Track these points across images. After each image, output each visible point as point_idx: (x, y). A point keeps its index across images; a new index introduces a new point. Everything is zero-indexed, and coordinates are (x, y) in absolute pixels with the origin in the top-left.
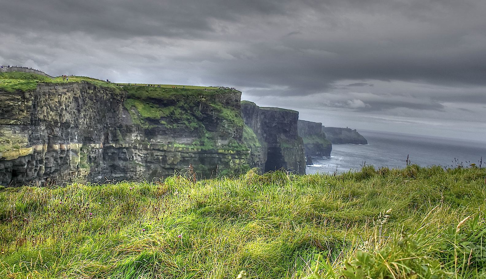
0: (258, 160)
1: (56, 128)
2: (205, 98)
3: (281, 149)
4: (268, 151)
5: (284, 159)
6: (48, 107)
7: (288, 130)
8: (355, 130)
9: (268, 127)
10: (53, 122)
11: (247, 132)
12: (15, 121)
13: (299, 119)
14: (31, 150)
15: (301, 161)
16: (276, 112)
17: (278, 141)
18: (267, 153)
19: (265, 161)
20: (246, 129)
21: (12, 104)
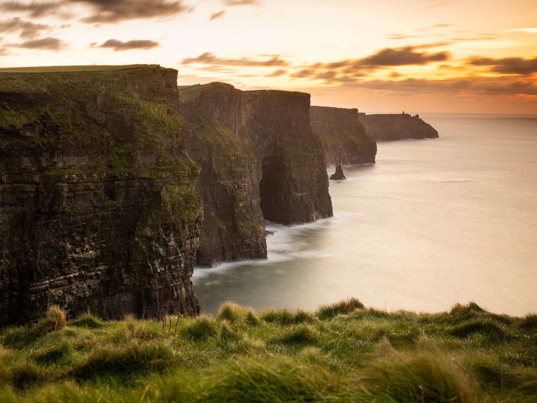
2: (106, 86)
4: (262, 162)
5: (290, 174)
7: (294, 125)
8: (417, 116)
11: (221, 136)
13: (311, 105)
17: (279, 144)
18: (261, 165)
19: (258, 179)
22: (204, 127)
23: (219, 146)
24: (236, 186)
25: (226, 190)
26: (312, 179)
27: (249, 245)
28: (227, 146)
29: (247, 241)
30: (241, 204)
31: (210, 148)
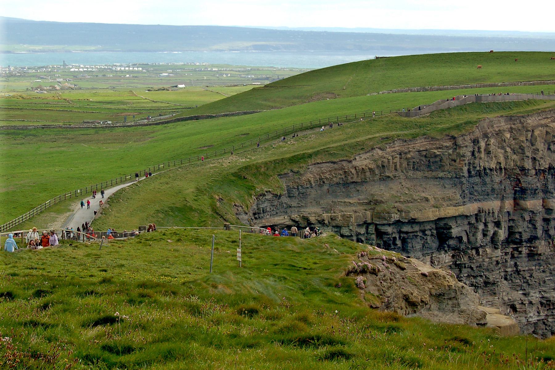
1: (525, 177)
6: (508, 149)
10: (518, 170)
12: (445, 173)
14: (471, 208)
21: (438, 153)
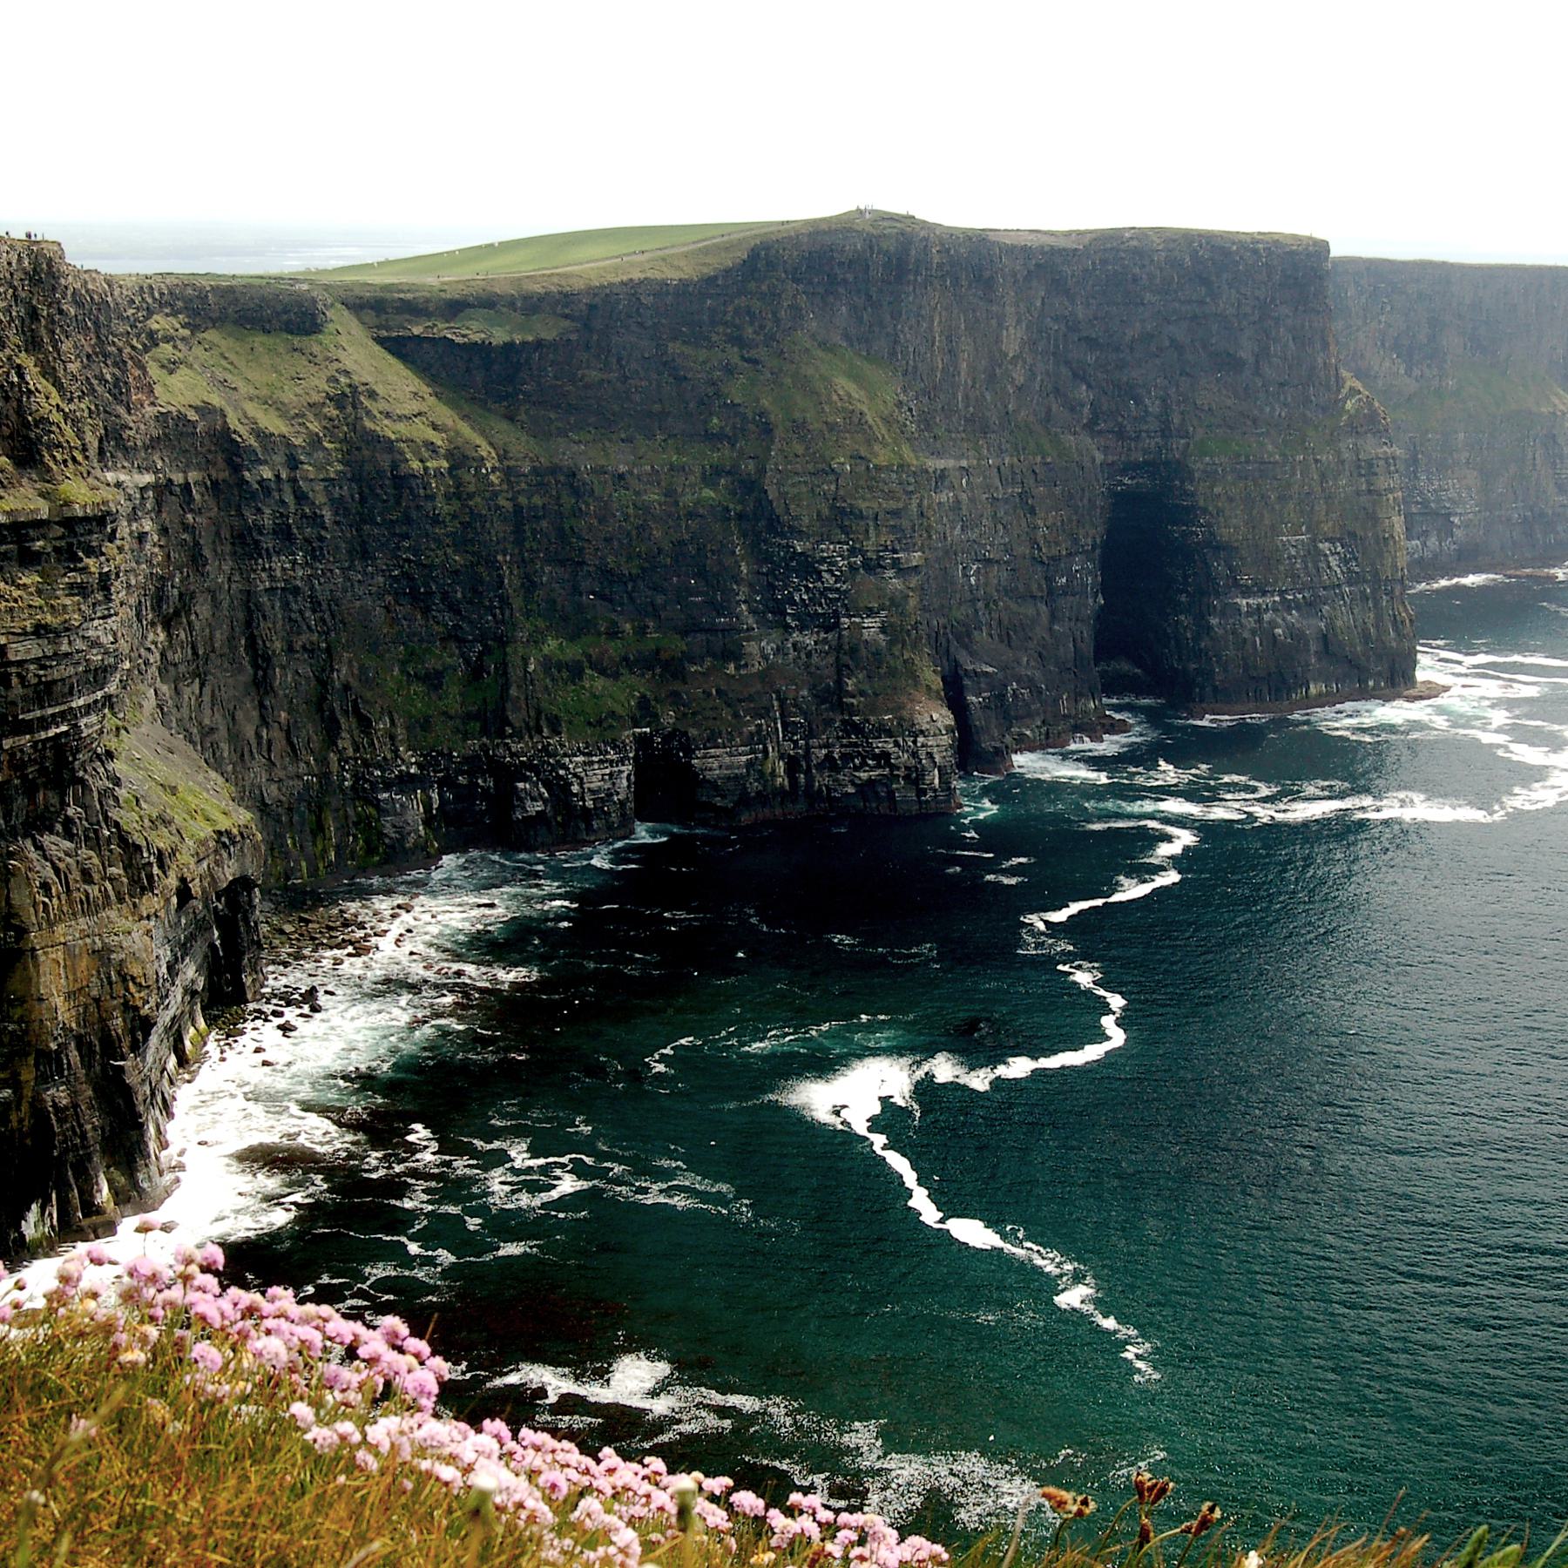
0: (887, 539)
3: (1191, 472)
7: (1246, 352)
9: (1091, 343)
15: (1353, 535)
16: (1137, 252)
20: (810, 371)
22: (755, 362)
23: (799, 428)
24: (858, 560)
25: (819, 573)
26: (1316, 547)
27: (886, 755)
28: (831, 427)
29: (884, 744)
30: (871, 625)
31: (767, 430)
